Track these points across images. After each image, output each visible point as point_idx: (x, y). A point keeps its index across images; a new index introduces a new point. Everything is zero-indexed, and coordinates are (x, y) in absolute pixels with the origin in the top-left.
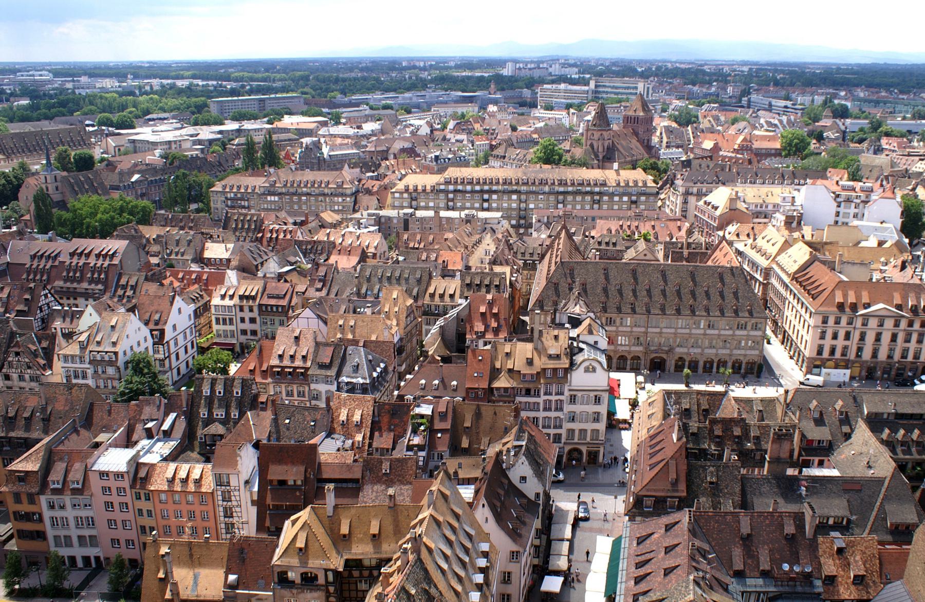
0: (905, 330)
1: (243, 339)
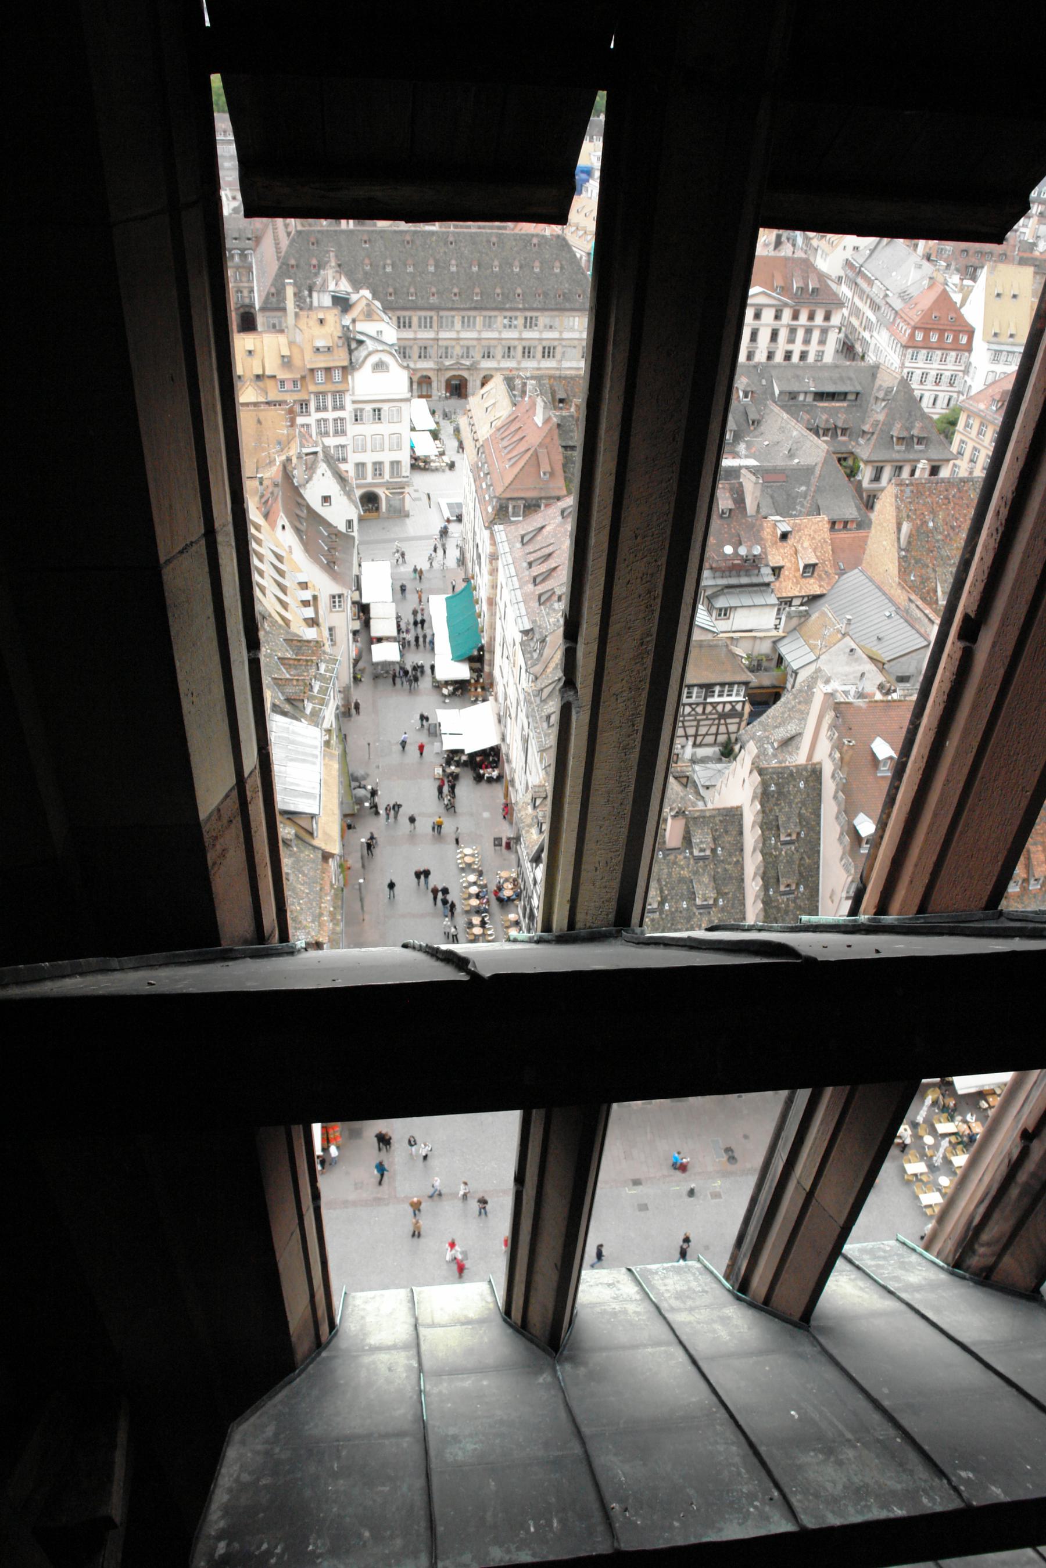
0: (788, 325)
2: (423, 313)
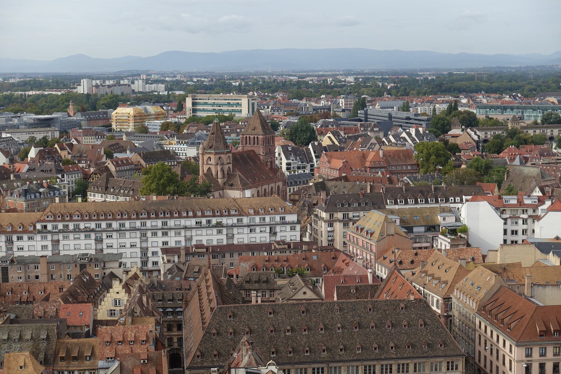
2: (316, 366)
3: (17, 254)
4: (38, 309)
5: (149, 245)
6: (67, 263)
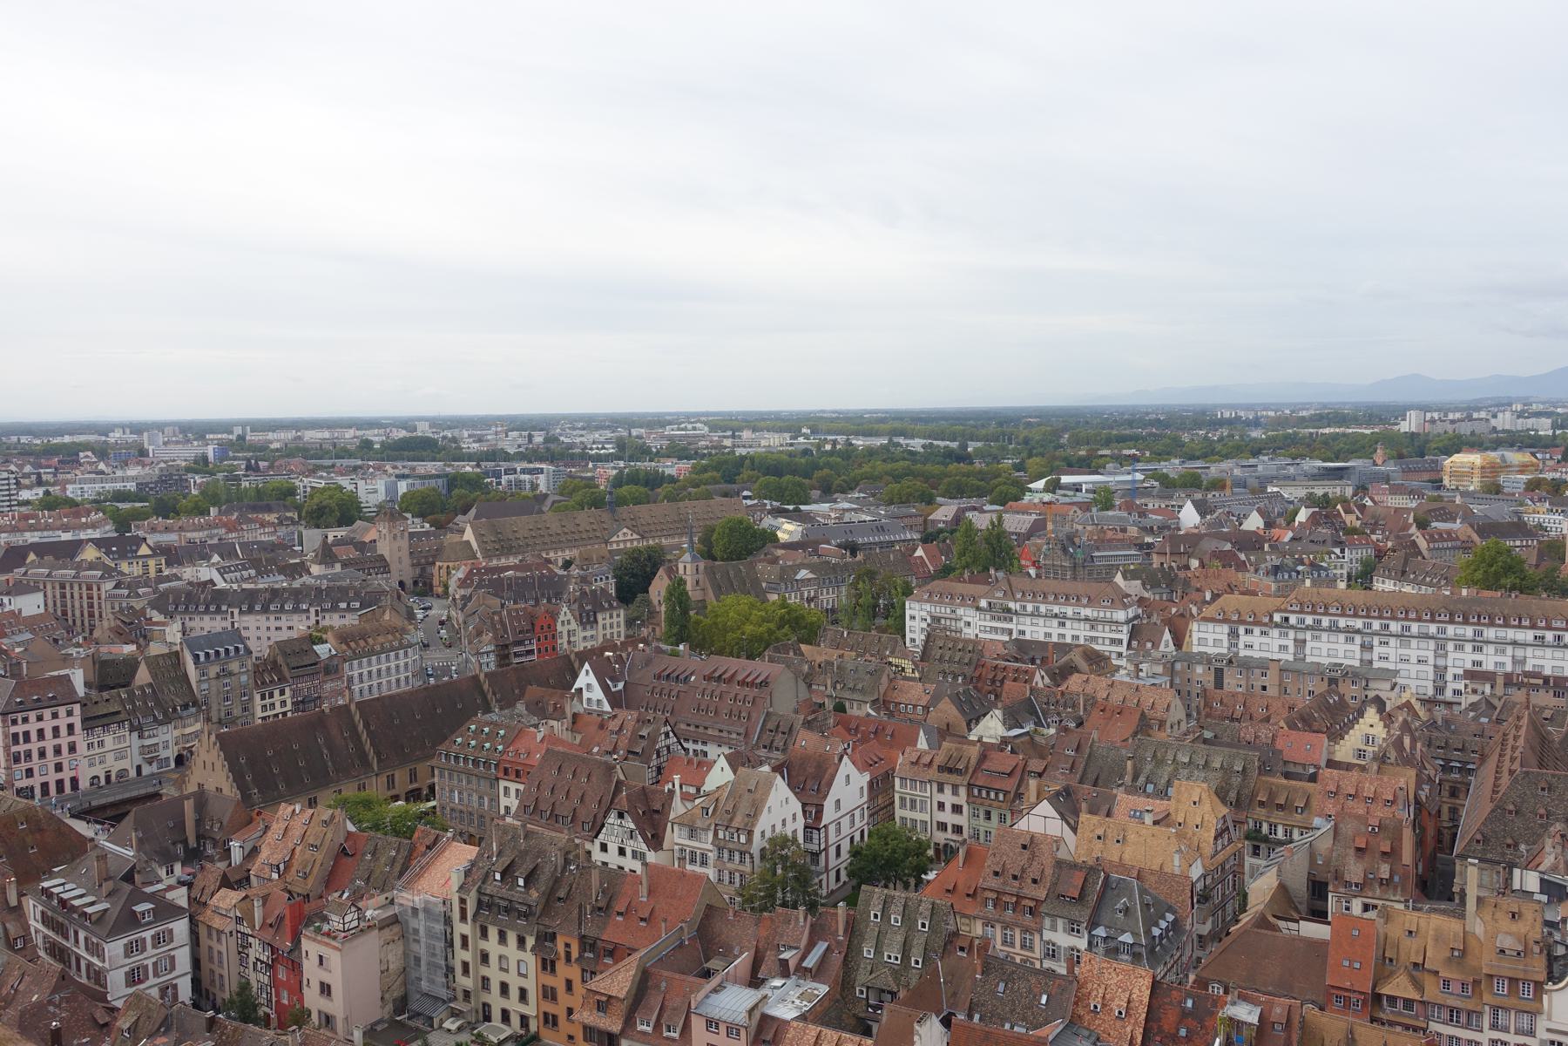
1: (940, 837)
3: (1242, 653)
4: (1247, 731)
5: (1450, 663)
6: (1309, 674)
